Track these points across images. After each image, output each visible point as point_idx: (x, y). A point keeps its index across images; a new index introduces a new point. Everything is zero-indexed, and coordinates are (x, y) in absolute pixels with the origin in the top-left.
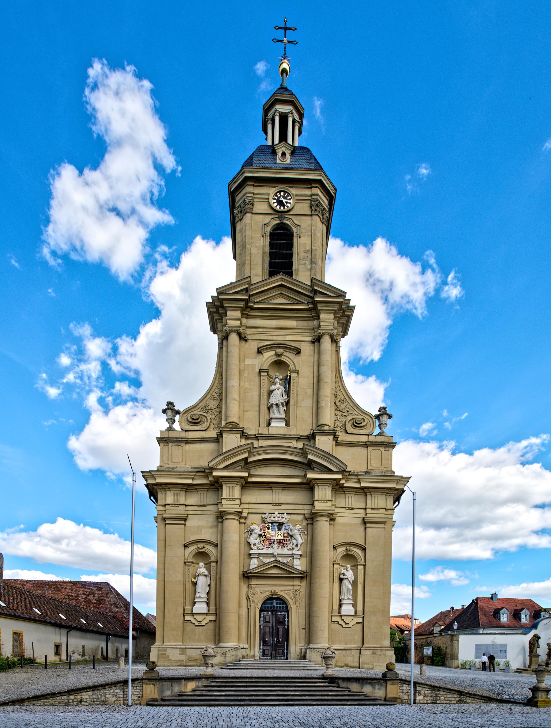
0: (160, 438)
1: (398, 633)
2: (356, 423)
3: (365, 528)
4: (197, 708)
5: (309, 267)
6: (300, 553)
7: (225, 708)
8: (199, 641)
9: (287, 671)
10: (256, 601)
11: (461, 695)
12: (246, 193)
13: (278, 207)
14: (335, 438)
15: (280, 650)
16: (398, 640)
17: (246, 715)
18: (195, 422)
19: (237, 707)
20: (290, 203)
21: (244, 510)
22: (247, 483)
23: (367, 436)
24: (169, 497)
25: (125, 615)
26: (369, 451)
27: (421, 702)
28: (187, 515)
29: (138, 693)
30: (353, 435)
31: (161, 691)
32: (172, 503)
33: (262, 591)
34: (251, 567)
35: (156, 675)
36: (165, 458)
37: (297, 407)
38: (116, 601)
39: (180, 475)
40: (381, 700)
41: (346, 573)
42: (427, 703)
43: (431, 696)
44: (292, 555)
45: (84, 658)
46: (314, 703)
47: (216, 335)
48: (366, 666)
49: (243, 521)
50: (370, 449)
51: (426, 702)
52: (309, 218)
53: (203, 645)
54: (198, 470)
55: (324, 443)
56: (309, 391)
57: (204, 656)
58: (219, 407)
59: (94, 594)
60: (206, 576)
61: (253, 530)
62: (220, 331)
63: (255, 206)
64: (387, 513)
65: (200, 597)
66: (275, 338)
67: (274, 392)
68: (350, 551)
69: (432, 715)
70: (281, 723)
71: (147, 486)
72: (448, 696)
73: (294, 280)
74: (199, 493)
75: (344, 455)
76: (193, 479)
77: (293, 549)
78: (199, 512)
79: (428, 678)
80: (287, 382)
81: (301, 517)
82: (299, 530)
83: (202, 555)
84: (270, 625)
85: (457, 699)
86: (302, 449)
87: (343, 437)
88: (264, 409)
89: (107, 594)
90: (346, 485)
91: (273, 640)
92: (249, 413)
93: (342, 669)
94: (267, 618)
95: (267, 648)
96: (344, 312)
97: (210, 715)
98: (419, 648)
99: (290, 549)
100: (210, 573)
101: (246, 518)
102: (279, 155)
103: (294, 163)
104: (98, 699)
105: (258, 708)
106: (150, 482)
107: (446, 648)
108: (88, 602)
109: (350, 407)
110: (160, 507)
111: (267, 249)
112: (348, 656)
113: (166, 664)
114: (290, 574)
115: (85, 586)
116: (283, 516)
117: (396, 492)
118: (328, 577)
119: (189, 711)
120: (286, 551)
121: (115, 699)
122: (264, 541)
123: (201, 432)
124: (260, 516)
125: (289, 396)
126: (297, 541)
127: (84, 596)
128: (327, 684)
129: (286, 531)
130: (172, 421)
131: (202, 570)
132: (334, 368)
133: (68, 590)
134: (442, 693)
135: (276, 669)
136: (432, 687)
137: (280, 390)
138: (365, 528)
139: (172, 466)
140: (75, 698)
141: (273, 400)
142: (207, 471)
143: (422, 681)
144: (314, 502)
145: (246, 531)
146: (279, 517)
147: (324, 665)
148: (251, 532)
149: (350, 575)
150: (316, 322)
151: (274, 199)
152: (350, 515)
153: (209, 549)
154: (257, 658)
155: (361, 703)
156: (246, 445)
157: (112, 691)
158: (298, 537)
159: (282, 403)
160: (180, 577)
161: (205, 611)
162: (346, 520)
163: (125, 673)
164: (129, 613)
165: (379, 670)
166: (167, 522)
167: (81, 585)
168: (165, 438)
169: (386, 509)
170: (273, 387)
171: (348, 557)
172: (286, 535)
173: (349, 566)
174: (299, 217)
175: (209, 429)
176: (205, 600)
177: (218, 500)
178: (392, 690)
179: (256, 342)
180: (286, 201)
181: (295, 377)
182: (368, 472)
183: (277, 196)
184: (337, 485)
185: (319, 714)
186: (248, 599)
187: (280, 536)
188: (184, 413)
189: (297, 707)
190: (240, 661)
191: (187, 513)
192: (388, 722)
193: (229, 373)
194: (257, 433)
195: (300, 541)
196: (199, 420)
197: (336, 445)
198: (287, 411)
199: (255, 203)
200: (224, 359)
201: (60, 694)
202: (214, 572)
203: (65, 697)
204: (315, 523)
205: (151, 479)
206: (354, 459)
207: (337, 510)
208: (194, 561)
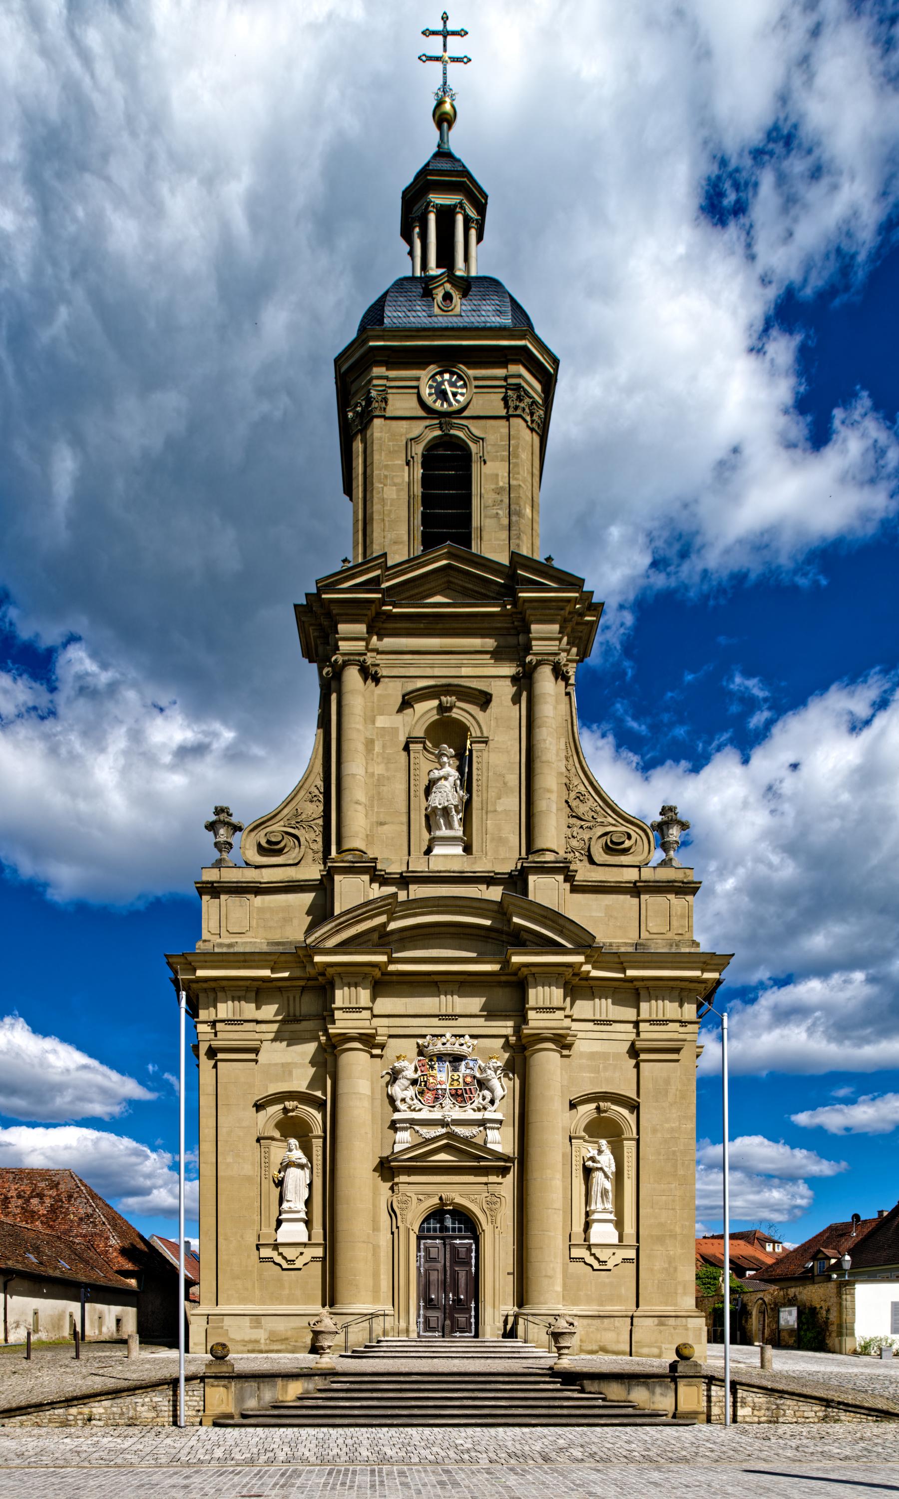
2: (612, 842)
5: (505, 521)
6: (499, 1116)
9: (477, 1361)
10: (409, 1216)
13: (439, 403)
15: (461, 1318)
20: (462, 394)
21: (380, 1031)
30: (607, 868)
41: (598, 1158)
44: (482, 1123)
46: (534, 1421)
47: (315, 666)
49: (376, 1052)
52: (504, 423)
63: (390, 402)
66: (437, 672)
68: (605, 1111)
77: (485, 1109)
80: (464, 762)
84: (439, 1266)
87: (584, 873)
88: (418, 820)
90: (595, 973)
92: (386, 827)
94: (434, 1253)
95: (435, 1315)
99: (479, 1110)
100: (310, 1160)
101: (382, 1046)
102: (439, 298)
103: (469, 314)
109: (598, 808)
111: (418, 490)
116: (462, 1040)
118: (559, 1166)
120: (471, 1115)
123: (288, 868)
125: (469, 790)
126: (492, 1091)
128: (558, 1386)
129: (468, 1071)
135: (454, 1357)
137: (451, 779)
144: (527, 1013)
148: (395, 1075)
150: (522, 638)
154: (414, 1335)
158: (495, 1083)
159: (456, 807)
160: (249, 1169)
161: (305, 1239)
162: (596, 1047)
168: (212, 883)
169: (680, 1021)
172: (469, 1080)
176: (303, 1215)
179: (398, 683)
180: (454, 390)
181: (481, 751)
182: (641, 945)
184: (574, 975)
186: (392, 1212)
187: (455, 1083)
188: (252, 830)
190: (379, 1342)
193: (345, 746)
194: (405, 869)
196: (282, 845)
198: (467, 822)
199: (390, 397)
206: (608, 920)
207: (575, 1026)
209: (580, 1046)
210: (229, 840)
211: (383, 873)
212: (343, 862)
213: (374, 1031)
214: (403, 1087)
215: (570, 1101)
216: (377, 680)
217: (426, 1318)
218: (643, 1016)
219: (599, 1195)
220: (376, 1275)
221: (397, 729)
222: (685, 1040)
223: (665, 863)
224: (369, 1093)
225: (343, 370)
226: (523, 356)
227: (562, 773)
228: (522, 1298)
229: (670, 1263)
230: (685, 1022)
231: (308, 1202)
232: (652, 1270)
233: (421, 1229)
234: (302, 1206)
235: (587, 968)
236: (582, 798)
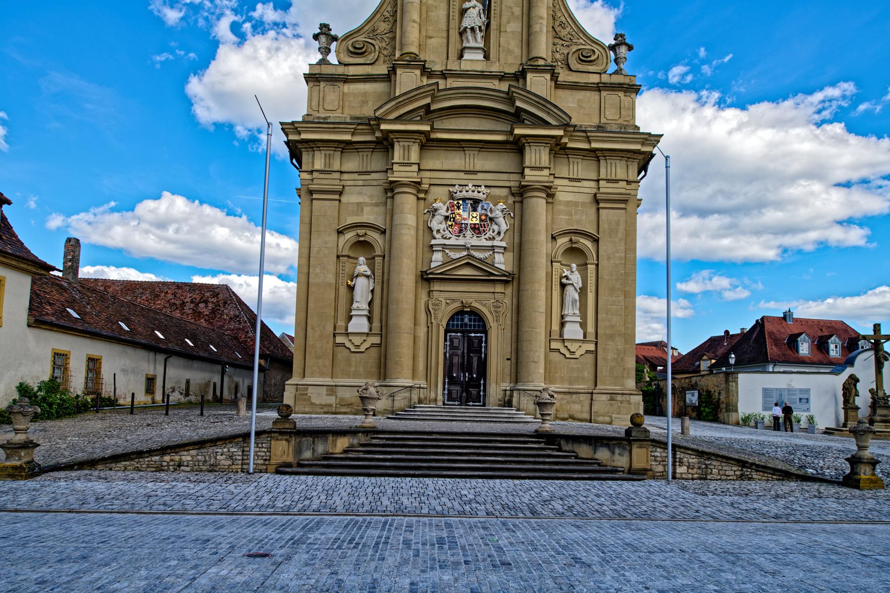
1: (647, 369)
2: (583, 56)
3: (598, 209)
4: (350, 479)
6: (504, 244)
7: (392, 479)
8: (356, 375)
9: (483, 424)
10: (440, 315)
11: (743, 467)
14: (554, 77)
15: (474, 391)
16: (648, 379)
17: (422, 491)
18: (357, 52)
19: (408, 479)
21: (424, 181)
22: (429, 140)
23: (598, 75)
25: (250, 334)
27: (684, 476)
29: (263, 454)
30: (579, 74)
31: (298, 451)
32: (323, 168)
34: (433, 265)
35: (292, 426)
36: (315, 103)
37: (500, 32)
38: (237, 313)
40: (623, 471)
41: (570, 276)
42: (693, 479)
43: (699, 468)
44: (493, 248)
45: (187, 399)
46: (523, 474)
48: (601, 419)
49: (422, 195)
50: (604, 93)
51: (690, 476)
53: (361, 382)
54: (359, 121)
55: (538, 83)
56: (517, 11)
57: (362, 398)
58: (392, 31)
59: (206, 302)
60: (368, 277)
61: (436, 210)
64: (628, 187)
65: (358, 309)
67: (469, 11)
69: (701, 497)
70: (474, 505)
71: (287, 143)
72: (725, 468)
74: (361, 154)
76: (353, 134)
77: (494, 238)
78: (361, 183)
79: (694, 439)
81: (504, 192)
83: (363, 245)
84: (460, 352)
85: (738, 473)
86: (508, 93)
87: (564, 76)
88: (454, 34)
89: (225, 303)
90: (570, 145)
91: (464, 376)
93: (566, 422)
95: (456, 389)
97: (370, 490)
98: (680, 393)
101: (426, 192)
104: (205, 461)
105: (441, 481)
106: (291, 137)
107: (719, 393)
108: (197, 314)
110: (305, 174)
112: (574, 402)
113: (307, 409)
114: (489, 277)
115: (194, 290)
116: (479, 189)
117: (641, 157)
118: (544, 281)
119: (338, 482)
121: (230, 462)
124: (446, 189)
125: (488, 17)
126: (499, 226)
127: (192, 305)
128: (542, 445)
129: (483, 212)
130: (326, 51)
131: (363, 268)
133: (170, 296)
134: (714, 463)
135: (467, 421)
136: (700, 454)
137: (477, 9)
138: (598, 209)
139: (323, 115)
140: (172, 460)
141: (467, 23)
142: (372, 123)
143: (685, 444)
146: (473, 191)
147: (539, 416)
149: (576, 278)
152: (576, 190)
153: (374, 236)
154: (440, 403)
155: (593, 475)
156: (428, 85)
157: (225, 450)
158: (501, 221)
159: (480, 27)
160: (331, 278)
161: (366, 330)
162: (570, 197)
163: (246, 422)
164: (255, 332)
165: (621, 425)
166: (315, 196)
167: (188, 288)
171: (574, 251)
172: (483, 217)
173: (574, 266)
176: (366, 313)
177: (387, 164)
178: (640, 457)
184: (557, 145)
185: (531, 492)
186: (428, 312)
188: (343, 40)
189: (498, 481)
190: (415, 407)
191: (343, 183)
192: (634, 506)
194: (444, 68)
195: (504, 227)
196: (363, 50)
197: (556, 88)
201: (151, 452)
202: (381, 271)
203: (157, 458)
204: (525, 201)
205: (293, 133)
206: (580, 108)
207: (557, 182)
208: (351, 255)
217: (449, 390)
218: (602, 176)
220: (414, 358)
223: (616, 73)
224: (415, 224)
228: (516, 377)
229: (618, 354)
231: (370, 304)
232: (606, 359)
233: (448, 325)
234: (366, 306)
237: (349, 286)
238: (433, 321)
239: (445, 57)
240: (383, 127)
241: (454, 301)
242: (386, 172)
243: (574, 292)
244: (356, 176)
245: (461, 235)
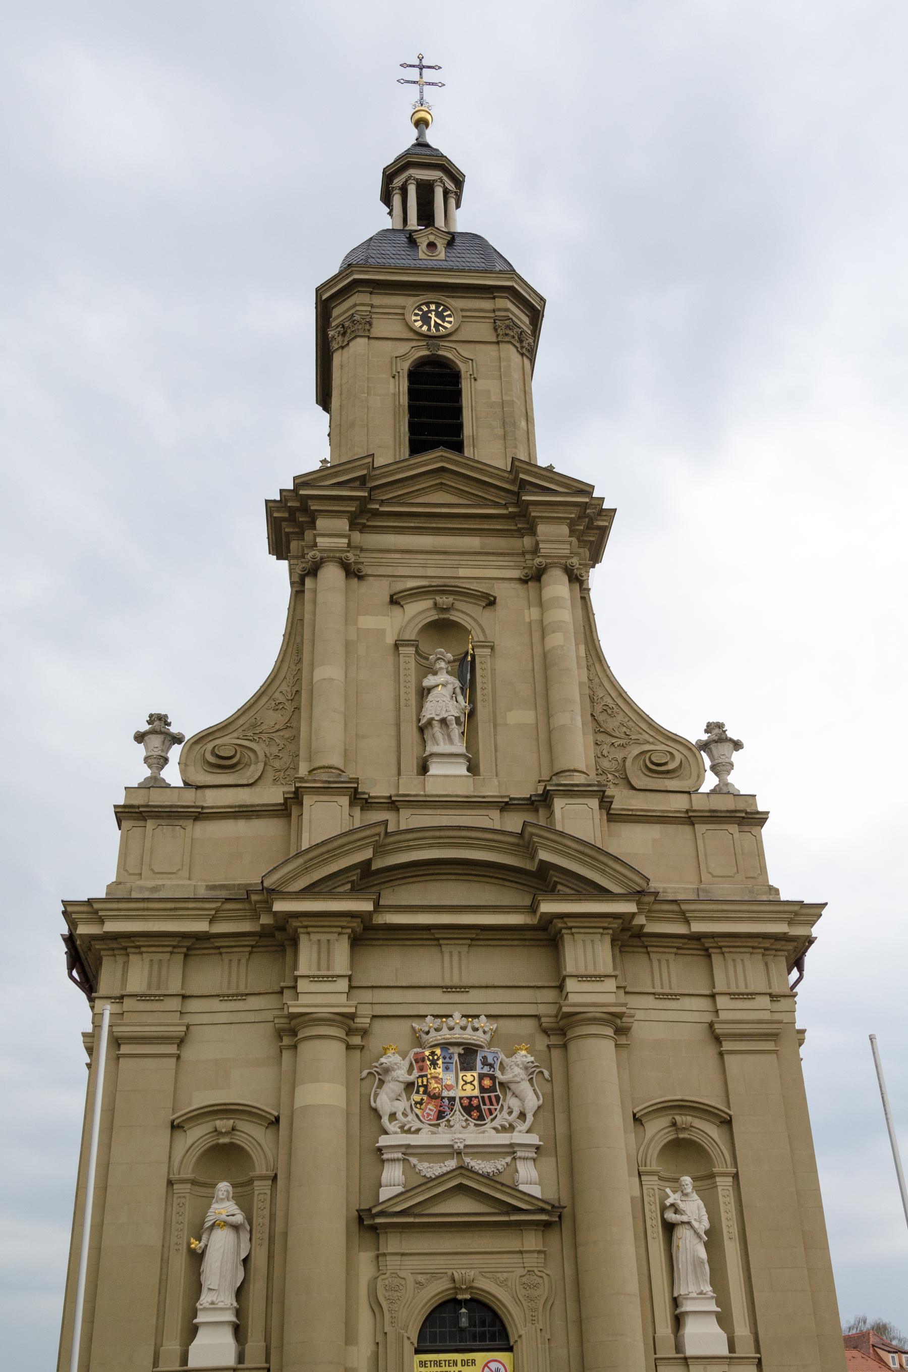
0: (124, 806)
5: (500, 432)
6: (534, 1139)
12: (355, 305)
14: (605, 803)
18: (224, 763)
20: (450, 322)
23: (686, 796)
24: (137, 975)
26: (699, 835)
28: (188, 1027)
30: (648, 794)
33: (420, 1278)
34: (385, 1194)
37: (495, 726)
39: (175, 909)
41: (682, 1206)
44: (511, 1149)
47: (285, 564)
50: (700, 828)
52: (495, 347)
60: (236, 1228)
61: (387, 1071)
62: (297, 558)
63: (374, 325)
66: (430, 572)
67: (434, 693)
73: (470, 459)
74: (226, 958)
75: (634, 844)
76: (212, 921)
77: (512, 1128)
78: (224, 1018)
81: (528, 1026)
82: (526, 1068)
83: (225, 1156)
87: (622, 800)
88: (410, 732)
96: (591, 520)
99: (504, 1129)
101: (365, 1033)
102: (423, 246)
103: (453, 259)
111: (404, 400)
117: (790, 946)
118: (630, 1220)
120: (488, 1136)
122: (421, 1103)
124: (405, 1024)
125: (472, 701)
126: (522, 1100)
129: (486, 1070)
130: (158, 761)
132: (581, 637)
137: (450, 687)
138: (721, 1054)
139: (151, 883)
145: (365, 1073)
146: (464, 1028)
149: (694, 1209)
151: (416, 315)
153: (252, 1135)
159: (457, 719)
160: (153, 1236)
166: (125, 1049)
169: (770, 995)
170: (429, 681)
171: (683, 1150)
172: (487, 1082)
173: (687, 1180)
174: (472, 346)
175: (260, 783)
179: (385, 583)
181: (485, 656)
183: (421, 310)
186: (376, 1307)
187: (468, 1087)
191: (187, 1019)
194: (393, 793)
195: (532, 1102)
197: (609, 821)
199: (375, 322)
200: (307, 617)
204: (572, 1046)
205: (87, 921)
208: (202, 1179)
209: (641, 1031)
210: (163, 754)
211: (366, 796)
212: (315, 781)
213: (353, 1010)
214: (393, 1095)
215: (634, 1115)
216: (361, 578)
219: (690, 1268)
221: (384, 630)
222: (780, 1022)
225: (324, 297)
226: (511, 292)
227: (583, 683)
230: (777, 996)
235: (640, 920)
236: (609, 711)
237: (192, 1252)
238: (388, 1329)
239: (394, 770)
240: (279, 906)
241: (434, 1275)
242: (281, 993)
243: (696, 1241)
244: (215, 1005)
245: (443, 1122)
